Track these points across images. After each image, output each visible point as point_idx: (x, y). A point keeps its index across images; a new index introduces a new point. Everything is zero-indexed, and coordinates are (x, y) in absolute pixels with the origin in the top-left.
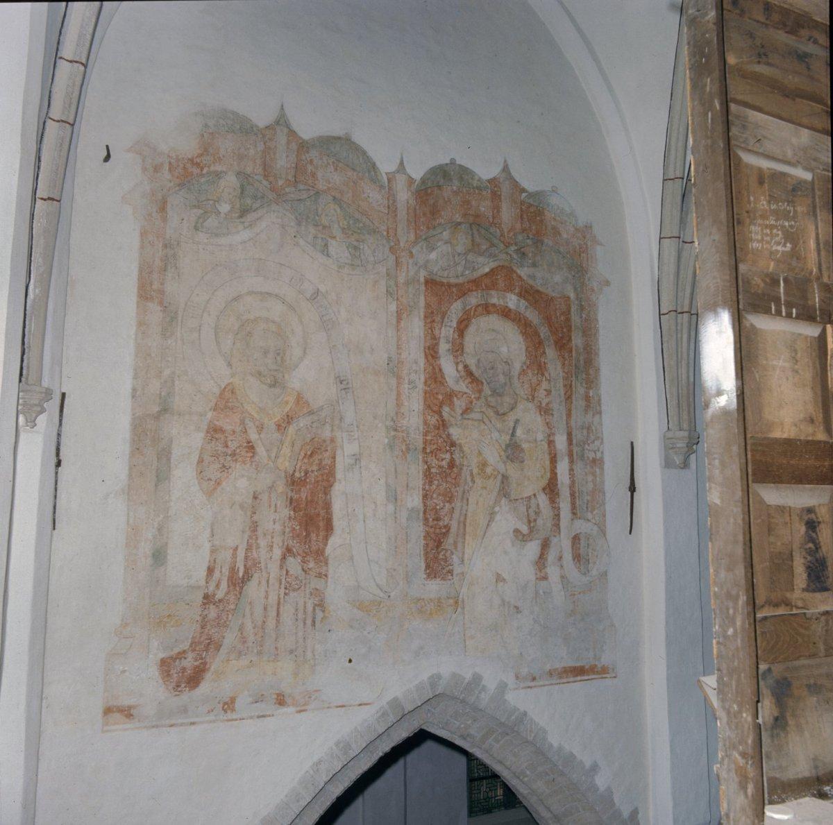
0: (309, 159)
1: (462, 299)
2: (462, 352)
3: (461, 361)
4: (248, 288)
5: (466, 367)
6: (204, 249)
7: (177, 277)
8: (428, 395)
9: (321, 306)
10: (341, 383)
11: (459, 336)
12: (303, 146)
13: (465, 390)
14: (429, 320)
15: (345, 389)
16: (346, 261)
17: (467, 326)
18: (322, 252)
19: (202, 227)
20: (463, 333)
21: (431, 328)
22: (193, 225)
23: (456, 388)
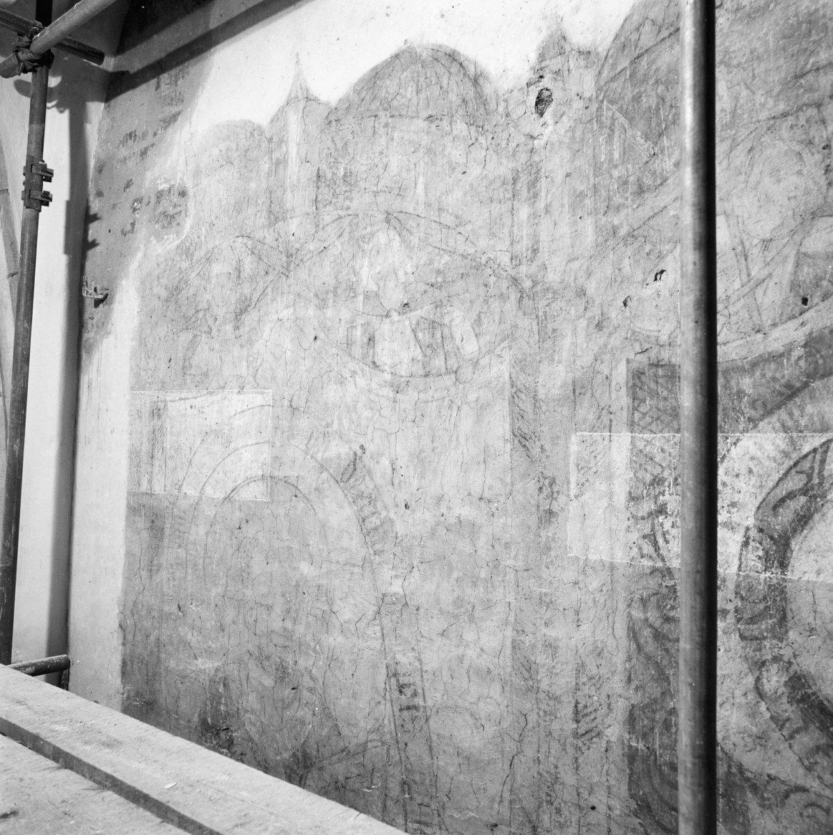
1: (782, 414)
2: (783, 618)
3: (776, 659)
4: (246, 471)
5: (798, 684)
7: (164, 468)
8: (639, 766)
9: (361, 496)
10: (401, 692)
11: (767, 559)
12: (330, 122)
13: (798, 776)
14: (647, 506)
15: (408, 708)
17: (803, 520)
20: (787, 545)
21: (651, 538)
23: (752, 761)
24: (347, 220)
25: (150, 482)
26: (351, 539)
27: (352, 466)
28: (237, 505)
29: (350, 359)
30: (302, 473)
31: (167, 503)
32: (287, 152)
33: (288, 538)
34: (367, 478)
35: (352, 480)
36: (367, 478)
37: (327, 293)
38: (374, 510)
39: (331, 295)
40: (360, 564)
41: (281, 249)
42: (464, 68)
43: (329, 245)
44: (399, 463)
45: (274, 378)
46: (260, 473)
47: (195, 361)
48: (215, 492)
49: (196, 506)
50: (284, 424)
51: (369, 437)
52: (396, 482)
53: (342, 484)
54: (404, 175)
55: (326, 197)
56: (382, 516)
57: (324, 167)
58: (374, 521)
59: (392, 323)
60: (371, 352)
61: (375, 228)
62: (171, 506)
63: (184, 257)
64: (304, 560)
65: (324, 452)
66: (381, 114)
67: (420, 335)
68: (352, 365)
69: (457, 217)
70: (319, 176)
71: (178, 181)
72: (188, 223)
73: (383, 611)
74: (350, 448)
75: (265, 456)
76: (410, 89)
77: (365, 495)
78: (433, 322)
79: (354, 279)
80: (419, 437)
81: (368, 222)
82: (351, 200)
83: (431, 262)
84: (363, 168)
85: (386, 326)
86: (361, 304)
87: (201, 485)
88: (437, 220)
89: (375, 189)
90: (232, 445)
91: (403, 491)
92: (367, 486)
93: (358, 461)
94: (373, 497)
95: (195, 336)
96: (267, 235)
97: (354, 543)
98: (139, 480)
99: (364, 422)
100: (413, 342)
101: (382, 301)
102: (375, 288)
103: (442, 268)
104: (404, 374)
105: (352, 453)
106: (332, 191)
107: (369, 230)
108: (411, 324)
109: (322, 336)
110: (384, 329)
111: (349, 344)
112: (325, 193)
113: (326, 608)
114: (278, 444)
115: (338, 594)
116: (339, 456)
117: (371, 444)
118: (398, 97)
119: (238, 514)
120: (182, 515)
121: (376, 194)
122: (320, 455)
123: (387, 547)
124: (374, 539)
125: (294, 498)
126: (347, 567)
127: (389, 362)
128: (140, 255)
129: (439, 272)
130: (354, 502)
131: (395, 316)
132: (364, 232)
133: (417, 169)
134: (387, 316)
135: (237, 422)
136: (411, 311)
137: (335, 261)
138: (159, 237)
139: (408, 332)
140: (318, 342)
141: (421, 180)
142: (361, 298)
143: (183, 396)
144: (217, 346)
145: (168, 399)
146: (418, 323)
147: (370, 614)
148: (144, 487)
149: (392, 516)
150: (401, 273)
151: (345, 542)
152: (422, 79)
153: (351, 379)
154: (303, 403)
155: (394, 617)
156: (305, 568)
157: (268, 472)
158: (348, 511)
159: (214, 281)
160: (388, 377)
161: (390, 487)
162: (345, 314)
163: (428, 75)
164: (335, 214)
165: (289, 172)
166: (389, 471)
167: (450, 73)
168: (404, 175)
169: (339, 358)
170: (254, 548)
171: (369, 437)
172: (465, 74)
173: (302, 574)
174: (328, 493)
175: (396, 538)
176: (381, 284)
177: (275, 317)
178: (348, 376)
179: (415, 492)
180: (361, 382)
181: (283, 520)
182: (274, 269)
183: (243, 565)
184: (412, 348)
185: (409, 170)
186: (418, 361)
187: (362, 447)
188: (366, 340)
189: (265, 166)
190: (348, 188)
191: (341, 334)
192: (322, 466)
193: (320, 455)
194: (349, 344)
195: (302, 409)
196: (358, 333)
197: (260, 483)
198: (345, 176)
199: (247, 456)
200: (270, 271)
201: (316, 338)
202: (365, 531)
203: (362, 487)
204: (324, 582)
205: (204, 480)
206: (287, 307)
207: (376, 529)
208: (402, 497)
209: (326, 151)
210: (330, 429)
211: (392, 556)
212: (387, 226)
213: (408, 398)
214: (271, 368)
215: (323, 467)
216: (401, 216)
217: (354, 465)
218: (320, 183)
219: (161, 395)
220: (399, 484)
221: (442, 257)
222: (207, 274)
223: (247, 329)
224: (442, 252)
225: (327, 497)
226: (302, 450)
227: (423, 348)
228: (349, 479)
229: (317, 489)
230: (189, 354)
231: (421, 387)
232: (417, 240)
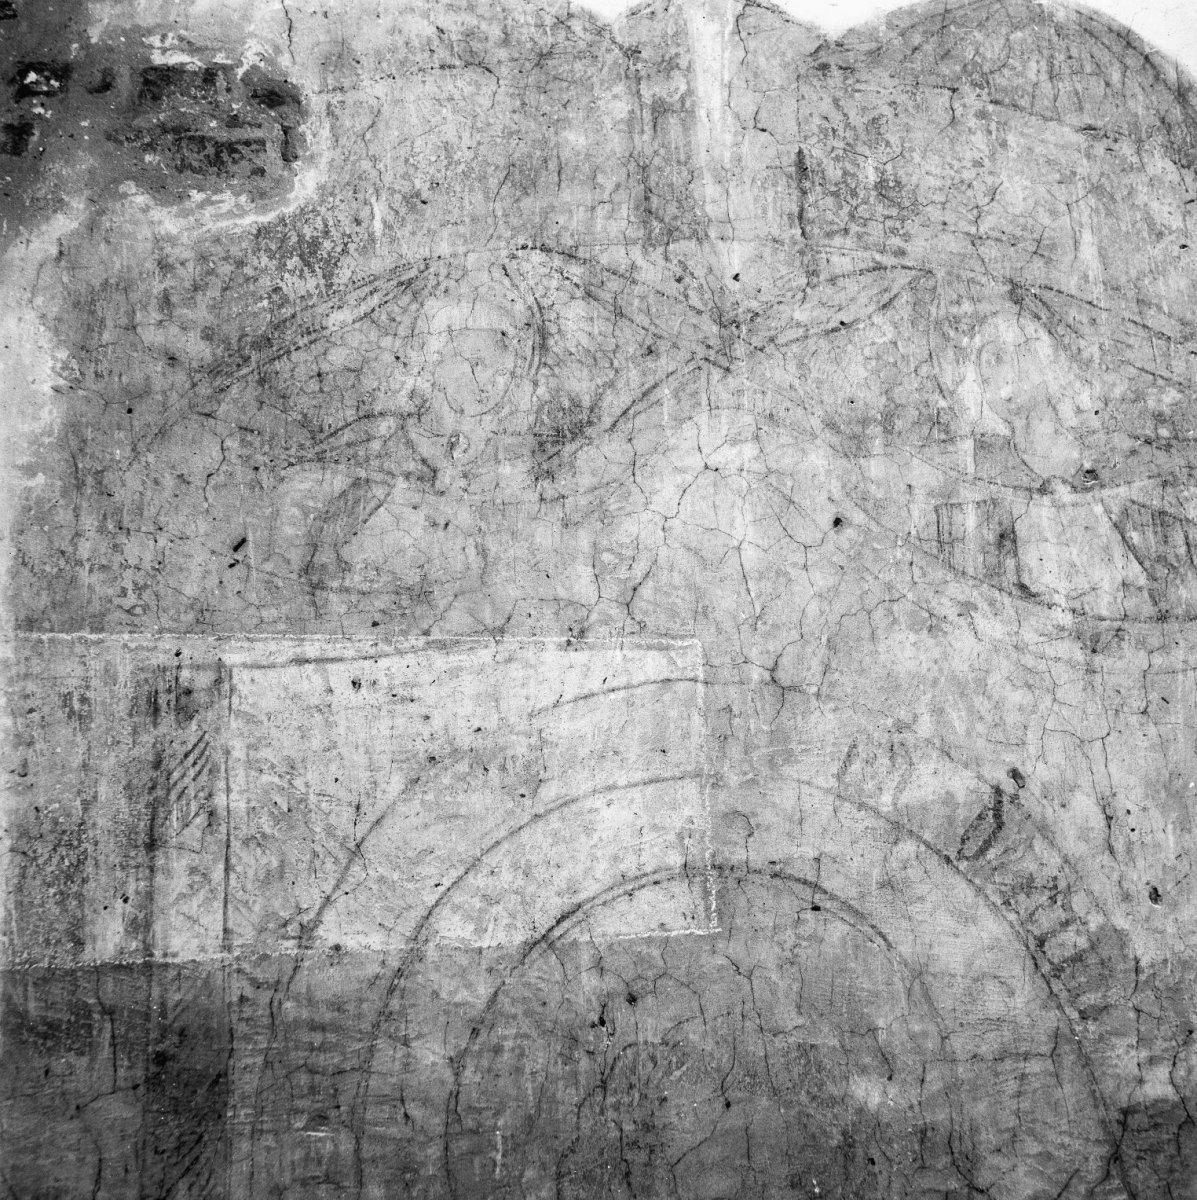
0: (858, 120)
6: (356, 684)
7: (218, 873)
9: (1028, 886)
12: (824, 67)
16: (1130, 604)
18: (993, 574)
19: (345, 567)
22: (296, 557)
24: (902, 279)
25: (140, 926)
26: (1011, 993)
27: (991, 819)
28: (586, 958)
29: (950, 576)
30: (830, 848)
31: (238, 987)
32: (690, 92)
33: (800, 1021)
34: (1039, 845)
35: (991, 854)
36: (1039, 845)
37: (865, 422)
38: (1063, 916)
39: (875, 430)
40: (1045, 1049)
41: (695, 301)
42: (1153, 67)
43: (856, 321)
44: (1122, 802)
45: (702, 613)
46: (675, 859)
47: (365, 550)
48: (480, 931)
49: (397, 979)
50: (759, 725)
51: (1032, 750)
52: (1119, 846)
53: (963, 865)
54: (1045, 219)
55: (830, 216)
56: (1093, 927)
57: (815, 152)
58: (1073, 940)
59: (1059, 507)
60: (1010, 563)
61: (984, 308)
62: (264, 997)
63: (293, 262)
64: (863, 1070)
65: (899, 789)
66: (966, 88)
67: (1135, 537)
68: (957, 590)
69: (1183, 323)
70: (801, 168)
71: (250, 59)
72: (306, 183)
73: (1129, 1153)
74: (979, 777)
75: (687, 812)
76: (1033, 65)
77: (1038, 883)
78: (1162, 513)
79: (943, 404)
80: (1163, 745)
81: (962, 292)
82: (907, 237)
83: (1139, 397)
84: (932, 181)
85: (1042, 512)
86: (970, 460)
87: (418, 913)
88: (1137, 319)
89: (973, 230)
90: (549, 792)
91: (1140, 863)
92: (1042, 862)
93: (1006, 807)
94: (1062, 885)
95: (356, 483)
96: (640, 262)
97: (1019, 1001)
98: (78, 923)
99: (1012, 718)
100: (1118, 550)
101: (1025, 457)
102: (1003, 430)
103: (1167, 411)
104: (1104, 613)
105: (987, 789)
106: (846, 209)
107: (967, 307)
108: (1108, 512)
109: (858, 517)
110: (1038, 518)
111: (945, 542)
112: (821, 205)
113: (953, 1184)
114: (733, 779)
115: (988, 1137)
116: (949, 799)
117: (1040, 765)
118: (1006, 71)
119: (589, 982)
120: (328, 1016)
121: (975, 240)
122: (886, 798)
123: (1115, 994)
124: (1073, 984)
125: (809, 915)
126: (1008, 1065)
127: (1063, 586)
128: (63, 225)
129: (1159, 418)
130: (1007, 903)
131: (1064, 493)
132: (954, 310)
133: (1075, 214)
134: (1043, 490)
135: (562, 727)
136: (1102, 486)
137: (878, 358)
138: (159, 188)
139: (1105, 527)
140: (849, 532)
141: (1087, 237)
142: (968, 445)
143: (311, 650)
144: (464, 517)
145: (231, 658)
146: (1125, 512)
147: (1093, 1168)
148: (109, 938)
149: (1121, 922)
150: (1066, 409)
151: (994, 1003)
152: (1061, 57)
153: (962, 621)
154: (812, 674)
155: (1161, 1160)
156: (869, 1092)
157: (702, 852)
158: (992, 927)
159: (435, 344)
160: (1067, 619)
161: (1106, 858)
162: (924, 474)
163: (1074, 52)
164: (866, 258)
165: (702, 135)
166: (1098, 821)
167: (1126, 67)
168: (1045, 219)
169: (917, 572)
170: (668, 1072)
171: (1032, 750)
172: (1157, 77)
173: (860, 1111)
174: (921, 889)
175: (1137, 970)
176: (1019, 423)
177: (696, 461)
178: (949, 610)
179: (1171, 861)
180: (993, 628)
181: (774, 977)
182: (675, 346)
183: (628, 1127)
184: (1119, 562)
185: (1053, 213)
186: (1140, 589)
187: (1015, 774)
188: (991, 537)
189: (616, 105)
190: (894, 212)
191: (918, 515)
192: (897, 826)
193: (886, 798)
194: (945, 542)
195: (814, 689)
196: (969, 520)
197: (679, 888)
198: (881, 186)
199: (614, 817)
200: (663, 346)
201: (837, 522)
202: (1046, 968)
203: (1028, 865)
204: (941, 1116)
205: (430, 899)
206: (734, 441)
207: (1078, 958)
208: (1140, 877)
209: (817, 120)
210: (907, 736)
211: (1132, 1015)
212: (1016, 308)
213: (1124, 664)
214: (692, 587)
215: (898, 828)
216: (1048, 296)
217: (998, 816)
218: (807, 184)
219: (196, 648)
220: (1129, 851)
221: (1161, 390)
222: (407, 320)
223: (586, 481)
224: (1160, 382)
225: (921, 899)
226: (828, 791)
227: (1147, 564)
228: (982, 851)
229: (887, 884)
230: (336, 529)
231: (1154, 641)
232: (1095, 349)
